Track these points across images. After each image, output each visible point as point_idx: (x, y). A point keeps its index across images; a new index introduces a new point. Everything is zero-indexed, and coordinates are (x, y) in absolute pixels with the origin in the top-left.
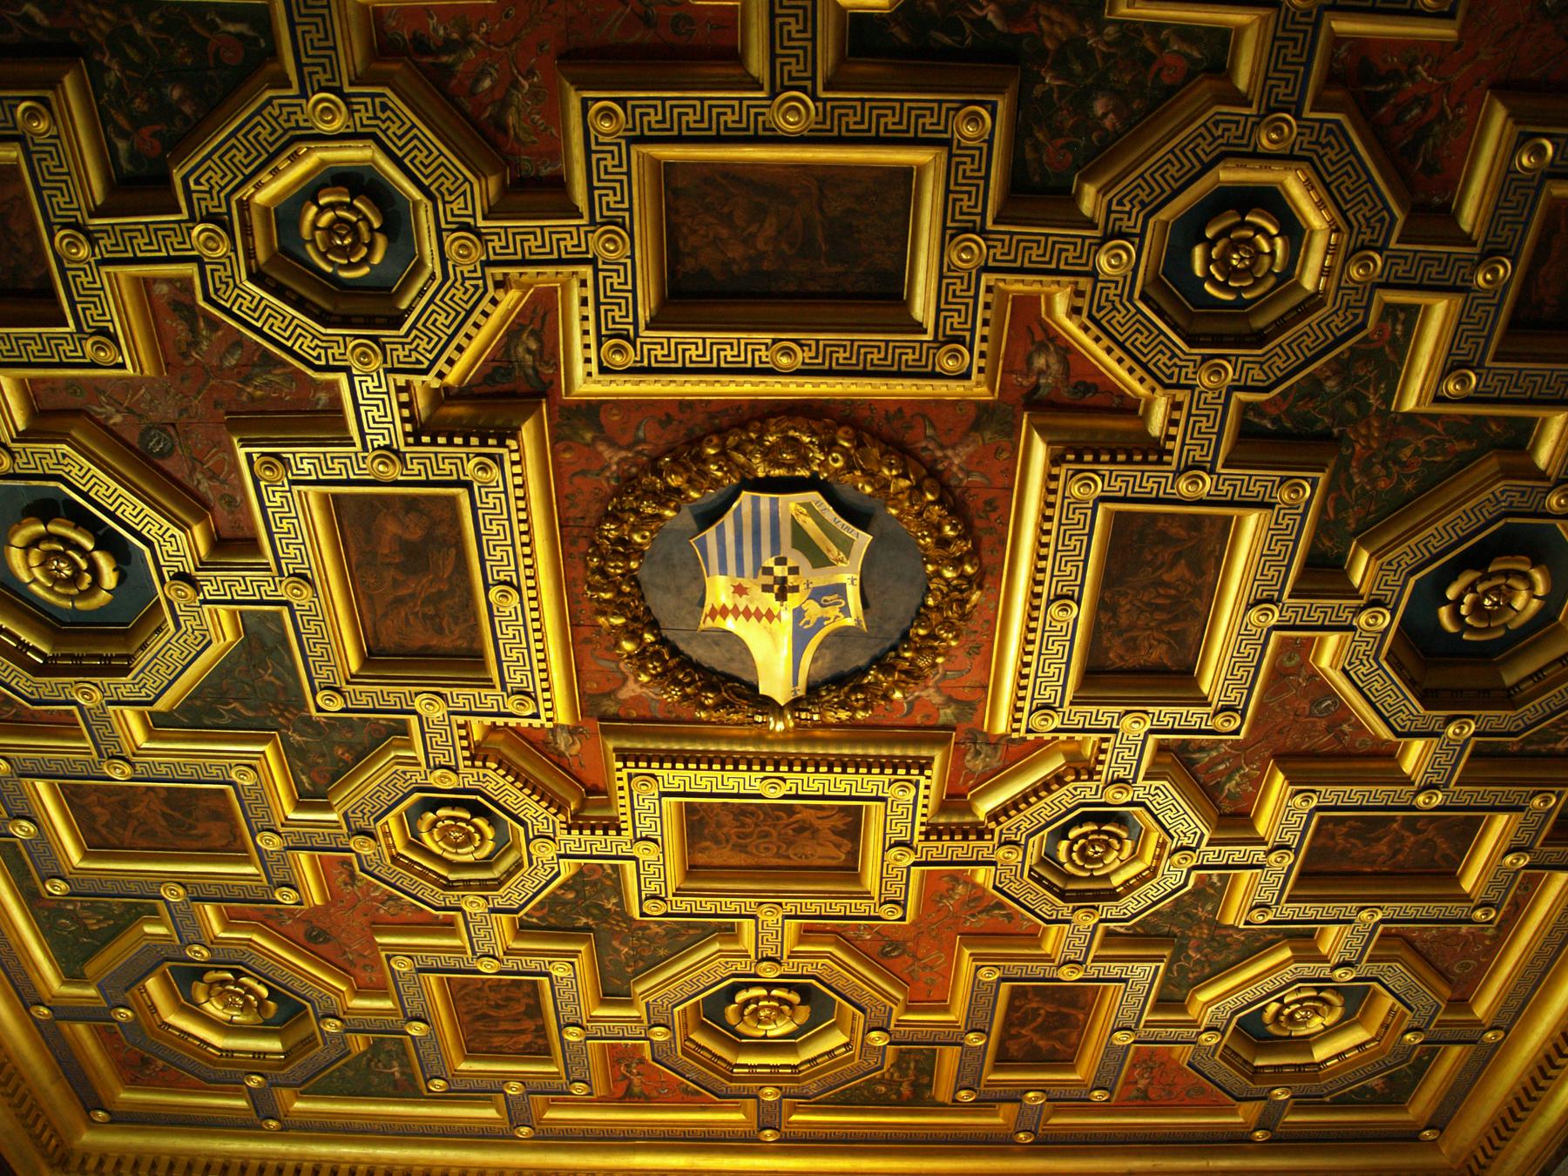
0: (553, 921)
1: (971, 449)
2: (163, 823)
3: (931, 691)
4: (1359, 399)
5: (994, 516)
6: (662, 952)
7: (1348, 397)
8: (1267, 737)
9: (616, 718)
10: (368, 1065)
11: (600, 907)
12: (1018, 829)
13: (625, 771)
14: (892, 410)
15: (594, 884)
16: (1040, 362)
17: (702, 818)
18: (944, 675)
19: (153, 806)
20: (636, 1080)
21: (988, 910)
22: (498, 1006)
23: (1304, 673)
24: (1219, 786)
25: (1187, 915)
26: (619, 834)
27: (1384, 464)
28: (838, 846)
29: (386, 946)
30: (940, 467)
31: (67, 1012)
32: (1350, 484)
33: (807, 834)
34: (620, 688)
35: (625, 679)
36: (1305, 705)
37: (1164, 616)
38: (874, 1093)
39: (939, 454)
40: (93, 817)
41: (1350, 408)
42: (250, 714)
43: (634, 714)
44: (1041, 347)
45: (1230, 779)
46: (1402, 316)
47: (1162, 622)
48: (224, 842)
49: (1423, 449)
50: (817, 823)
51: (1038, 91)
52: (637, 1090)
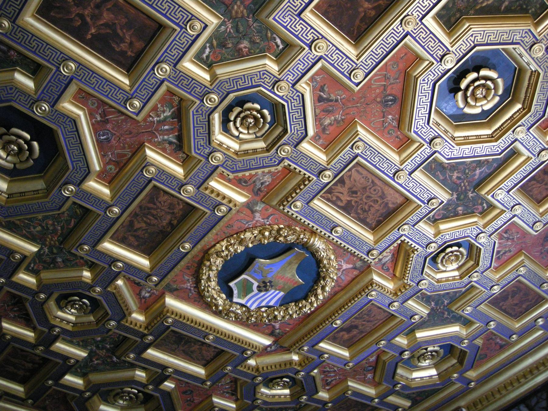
1: (183, 285)
3: (256, 219)
4: (51, 252)
5: (189, 265)
7: (55, 254)
8: (138, 134)
11: (458, 199)
12: (271, 160)
14: (196, 303)
16: (147, 295)
18: (247, 223)
21: (328, 100)
23: (108, 159)
24: (173, 116)
25: (237, 31)
27: (48, 229)
28: (350, 176)
30: (195, 285)
32: (62, 228)
33: (354, 189)
34: (349, 268)
35: (344, 270)
36: (114, 142)
37: (152, 211)
39: (192, 289)
41: (55, 251)
44: (144, 298)
45: (166, 118)
46: (30, 268)
47: (155, 209)
49: (32, 227)
50: (345, 193)
51: (112, 346)
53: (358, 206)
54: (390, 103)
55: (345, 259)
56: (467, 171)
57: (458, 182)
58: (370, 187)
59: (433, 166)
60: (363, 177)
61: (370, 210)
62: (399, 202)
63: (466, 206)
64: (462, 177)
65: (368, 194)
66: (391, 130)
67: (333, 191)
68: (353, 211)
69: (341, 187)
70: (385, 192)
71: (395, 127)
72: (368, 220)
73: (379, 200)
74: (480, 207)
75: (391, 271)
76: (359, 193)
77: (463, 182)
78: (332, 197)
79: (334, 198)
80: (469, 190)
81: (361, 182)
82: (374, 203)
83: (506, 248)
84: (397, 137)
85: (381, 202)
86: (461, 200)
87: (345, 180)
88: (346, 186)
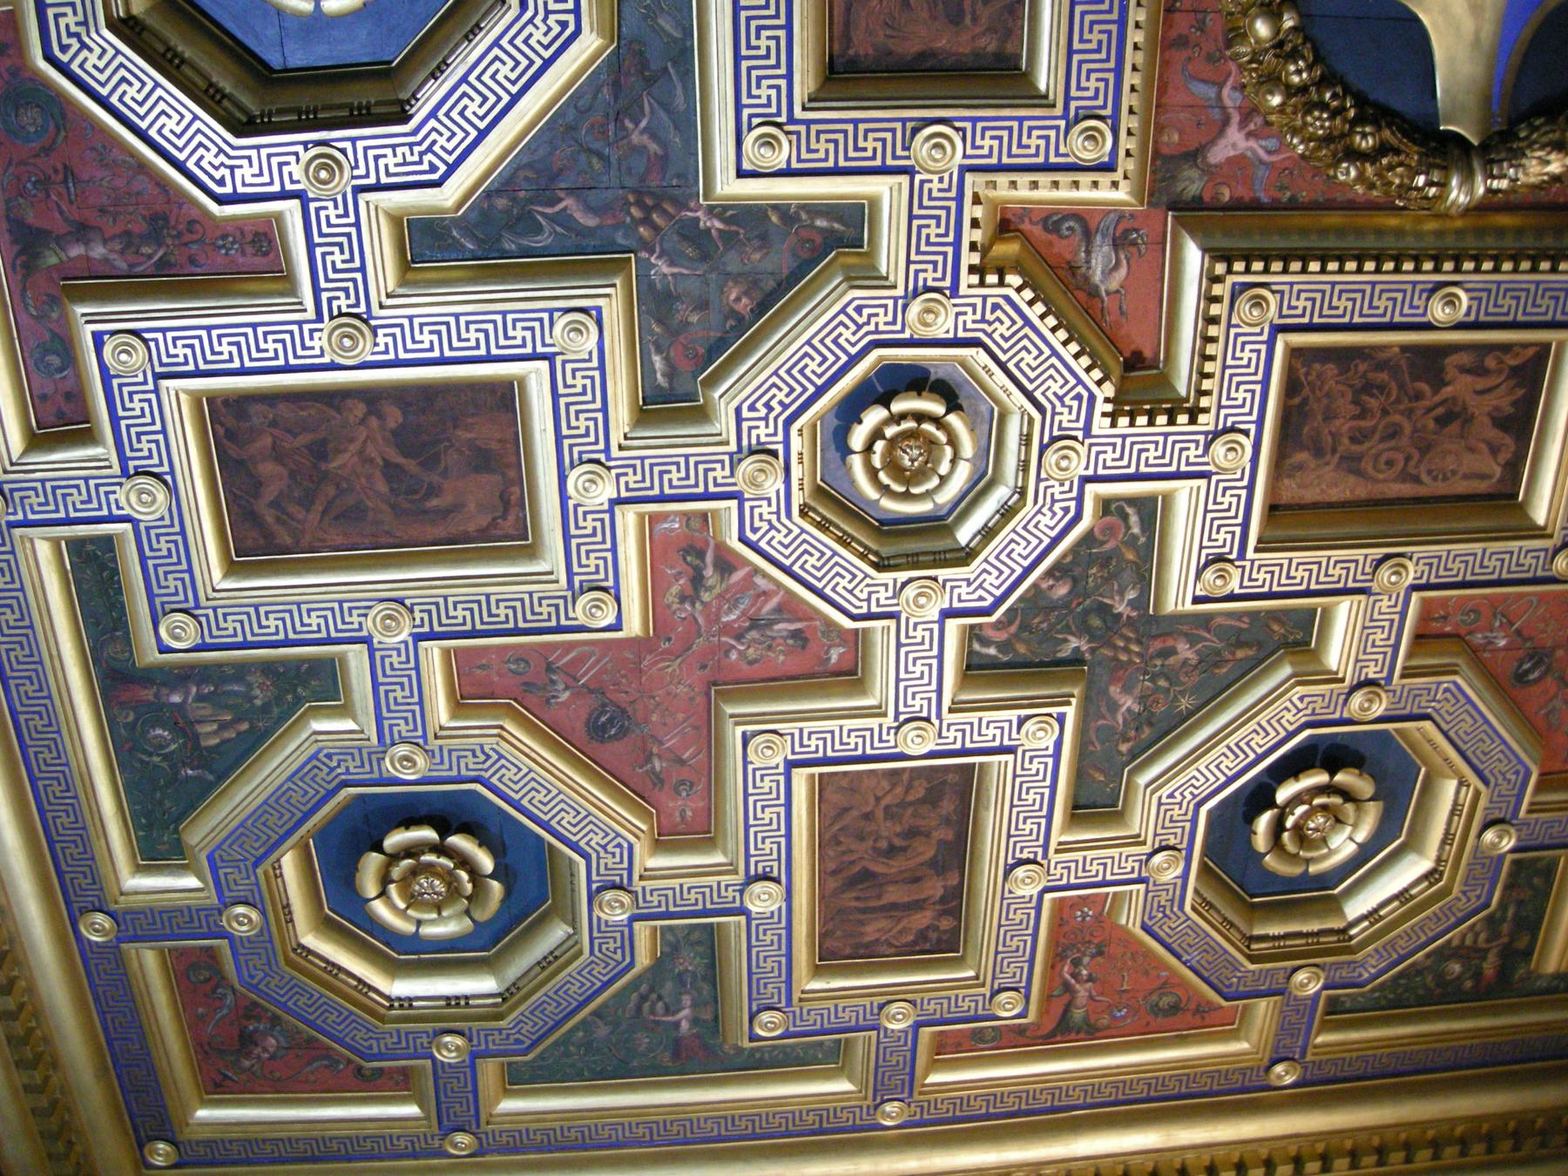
0: (1022, 649)
2: (382, 487)
6: (1185, 704)
9: (1197, 204)
10: (639, 1008)
11: (1104, 610)
13: (1230, 279)
15: (1105, 560)
17: (1305, 401)
19: (371, 451)
20: (1082, 991)
22: (892, 851)
26: (1193, 421)
28: (1494, 451)
29: (741, 719)
31: (143, 923)
33: (1454, 428)
34: (1213, 142)
35: (1226, 122)
38: (1440, 979)
40: (258, 485)
42: (590, 221)
43: (1226, 195)
48: (484, 521)
52: (1078, 1014)
53: (1401, 387)
54: (1526, 666)
55: (1261, 172)
56: (1162, 683)
57: (1157, 645)
58: (1413, 463)
59: (1276, 627)
60: (1454, 473)
61: (1355, 402)
62: (1286, 481)
63: (1054, 609)
64: (1159, 662)
65: (1404, 441)
66: (1475, 621)
67: (1512, 383)
68: (1403, 362)
69: (1497, 408)
70: (1352, 479)
71: (1471, 633)
72: (1331, 369)
73: (1355, 448)
74: (1002, 636)
75: (1037, 231)
76: (1431, 425)
77: (1138, 654)
78: (1501, 362)
79: (1490, 363)
80: (1092, 651)
81: (1450, 459)
82: (1360, 430)
83: (720, 596)
84: (1445, 618)
85: (1341, 449)
86: (1086, 612)
87: (1501, 434)
88: (1487, 420)
